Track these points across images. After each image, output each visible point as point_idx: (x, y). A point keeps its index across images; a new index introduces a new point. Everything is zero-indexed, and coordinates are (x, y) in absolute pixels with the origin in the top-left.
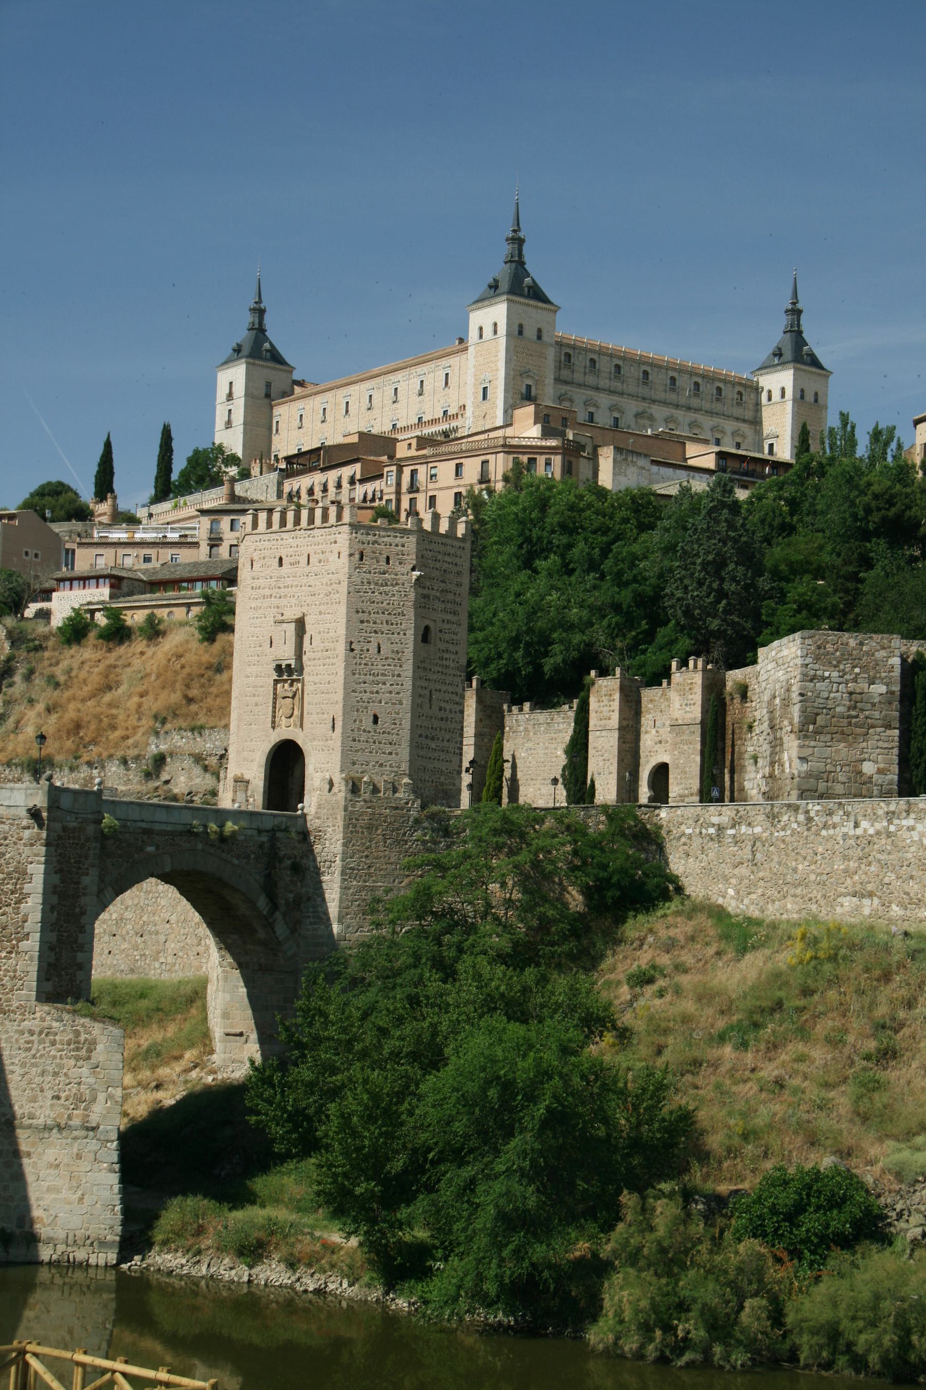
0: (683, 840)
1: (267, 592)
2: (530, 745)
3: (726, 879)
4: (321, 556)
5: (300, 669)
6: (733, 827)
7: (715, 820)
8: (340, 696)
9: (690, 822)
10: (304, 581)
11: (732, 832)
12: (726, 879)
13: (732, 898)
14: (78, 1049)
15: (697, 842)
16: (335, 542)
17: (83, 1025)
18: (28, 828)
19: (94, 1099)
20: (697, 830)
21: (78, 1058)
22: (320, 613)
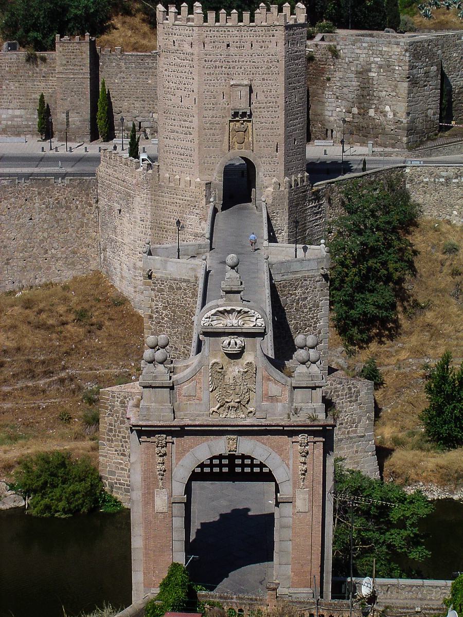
0: (422, 185)
1: (218, 64)
2: (122, 75)
3: (452, 206)
4: (262, 44)
5: (250, 116)
6: (456, 178)
7: (444, 174)
8: (282, 131)
9: (426, 175)
10: (249, 58)
11: (454, 181)
12: (452, 206)
13: (456, 216)
14: (351, 397)
15: (431, 186)
16: (273, 36)
17: (353, 384)
18: (319, 281)
19: (359, 422)
20: (432, 180)
21: (350, 402)
22: (263, 79)
